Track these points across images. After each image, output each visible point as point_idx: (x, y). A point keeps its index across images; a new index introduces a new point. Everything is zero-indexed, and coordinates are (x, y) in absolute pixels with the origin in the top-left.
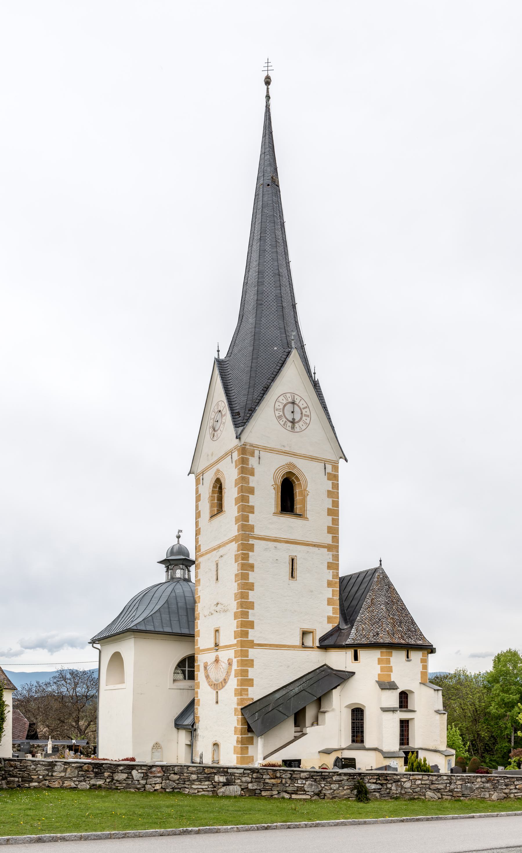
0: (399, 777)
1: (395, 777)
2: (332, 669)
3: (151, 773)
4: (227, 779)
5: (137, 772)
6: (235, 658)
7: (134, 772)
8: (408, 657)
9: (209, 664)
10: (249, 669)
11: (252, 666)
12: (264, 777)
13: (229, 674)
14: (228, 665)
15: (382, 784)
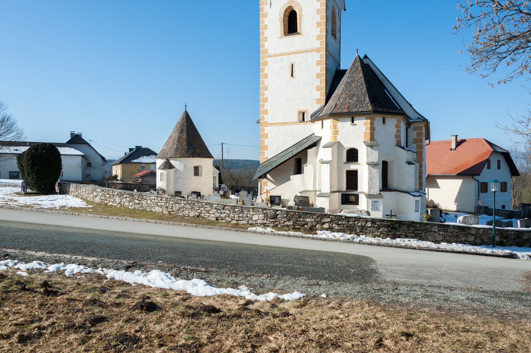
10: (265, 139)
11: (267, 138)
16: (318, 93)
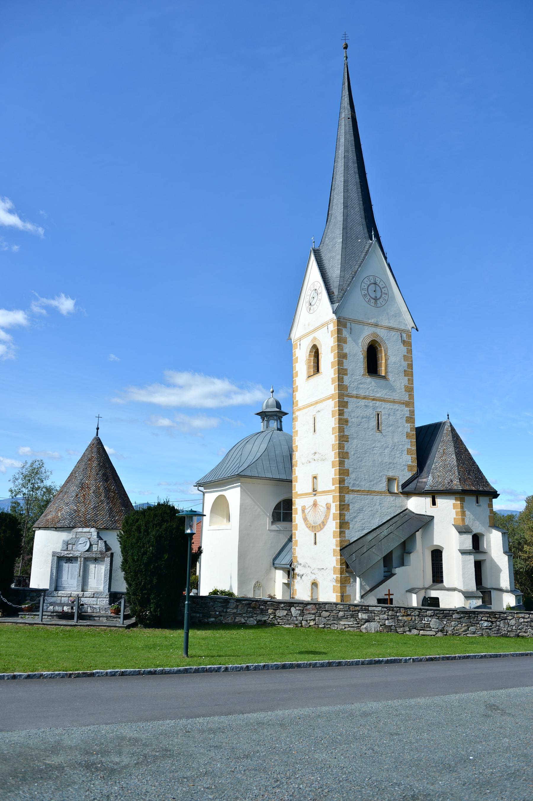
0: (505, 615)
1: (502, 615)
2: (413, 513)
3: (307, 610)
4: (368, 616)
5: (295, 609)
6: (333, 502)
7: (293, 609)
8: (477, 503)
9: (307, 507)
10: (346, 513)
11: (348, 510)
12: (398, 614)
13: (327, 517)
14: (326, 509)
15: (492, 622)
16: (409, 457)
